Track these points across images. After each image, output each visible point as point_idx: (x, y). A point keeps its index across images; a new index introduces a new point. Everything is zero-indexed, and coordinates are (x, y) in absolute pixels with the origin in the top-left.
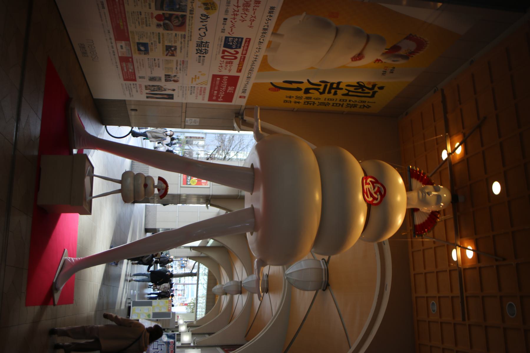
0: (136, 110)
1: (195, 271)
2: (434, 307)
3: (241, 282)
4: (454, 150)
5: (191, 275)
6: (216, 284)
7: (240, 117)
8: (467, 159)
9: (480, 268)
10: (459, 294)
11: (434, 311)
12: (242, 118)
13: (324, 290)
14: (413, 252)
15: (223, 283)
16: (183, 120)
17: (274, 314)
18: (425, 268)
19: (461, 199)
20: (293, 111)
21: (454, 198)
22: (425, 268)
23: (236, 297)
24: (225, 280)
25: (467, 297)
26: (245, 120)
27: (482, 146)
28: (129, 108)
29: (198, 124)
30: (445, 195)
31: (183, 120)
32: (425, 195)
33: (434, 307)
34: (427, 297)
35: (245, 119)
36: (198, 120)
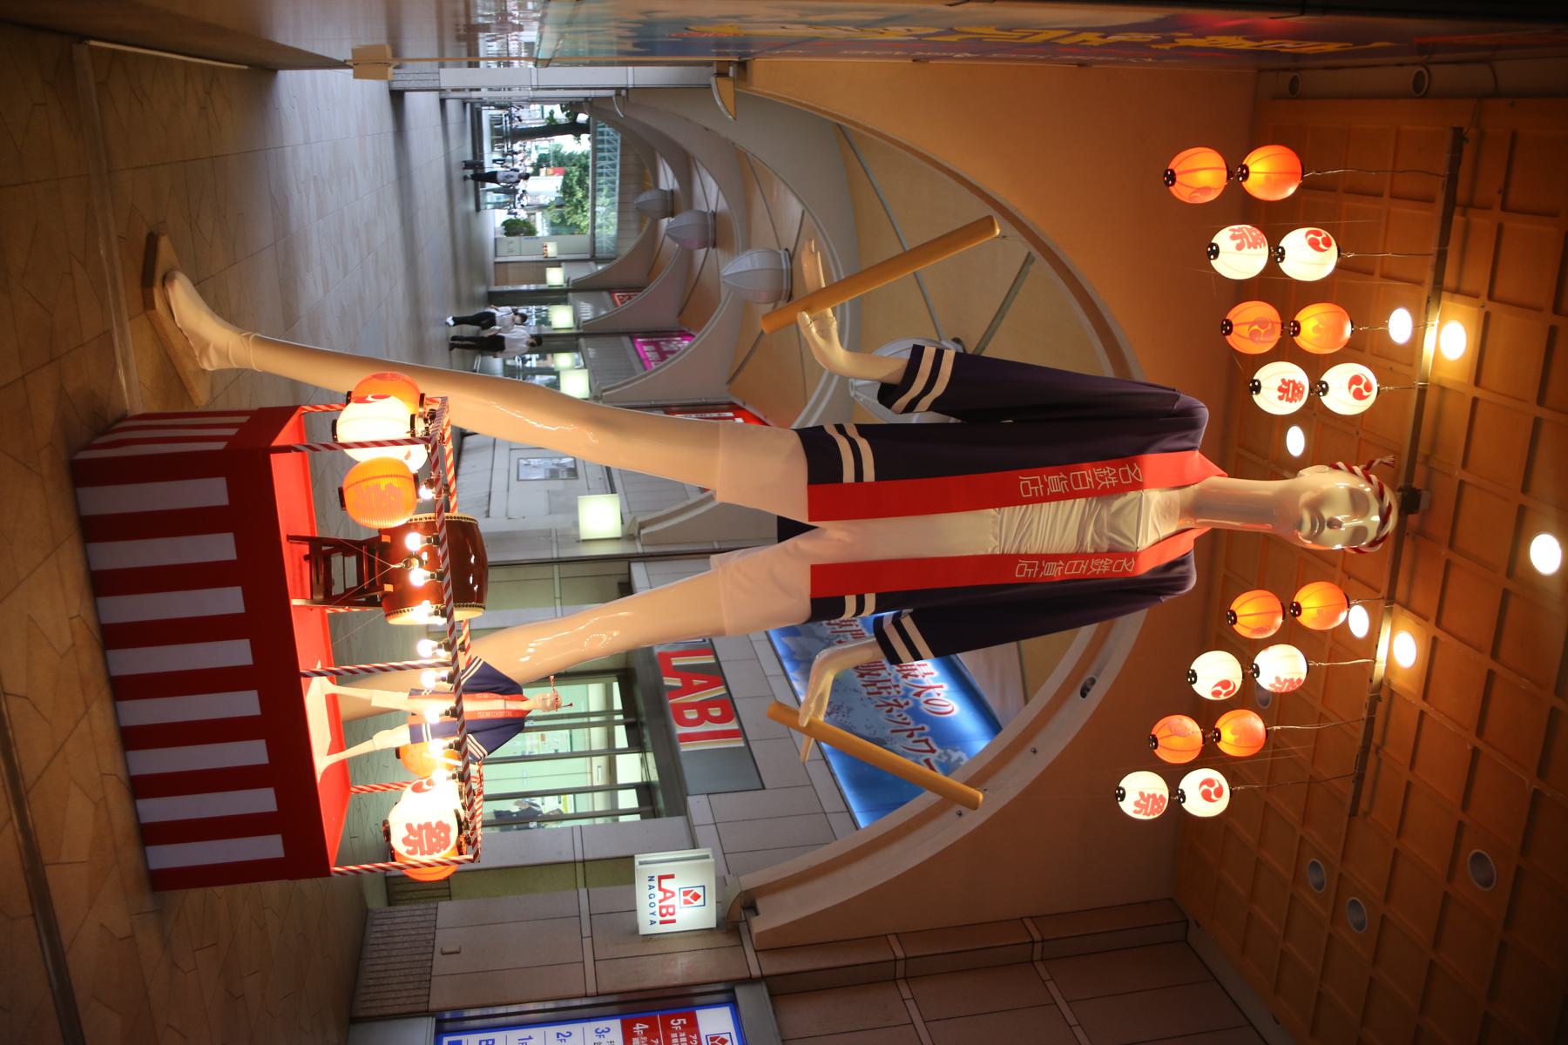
1: (582, 118)
3: (714, 215)
5: (575, 129)
6: (642, 189)
9: (1422, 713)
15: (663, 186)
23: (702, 252)
24: (667, 180)
32: (1321, 529)
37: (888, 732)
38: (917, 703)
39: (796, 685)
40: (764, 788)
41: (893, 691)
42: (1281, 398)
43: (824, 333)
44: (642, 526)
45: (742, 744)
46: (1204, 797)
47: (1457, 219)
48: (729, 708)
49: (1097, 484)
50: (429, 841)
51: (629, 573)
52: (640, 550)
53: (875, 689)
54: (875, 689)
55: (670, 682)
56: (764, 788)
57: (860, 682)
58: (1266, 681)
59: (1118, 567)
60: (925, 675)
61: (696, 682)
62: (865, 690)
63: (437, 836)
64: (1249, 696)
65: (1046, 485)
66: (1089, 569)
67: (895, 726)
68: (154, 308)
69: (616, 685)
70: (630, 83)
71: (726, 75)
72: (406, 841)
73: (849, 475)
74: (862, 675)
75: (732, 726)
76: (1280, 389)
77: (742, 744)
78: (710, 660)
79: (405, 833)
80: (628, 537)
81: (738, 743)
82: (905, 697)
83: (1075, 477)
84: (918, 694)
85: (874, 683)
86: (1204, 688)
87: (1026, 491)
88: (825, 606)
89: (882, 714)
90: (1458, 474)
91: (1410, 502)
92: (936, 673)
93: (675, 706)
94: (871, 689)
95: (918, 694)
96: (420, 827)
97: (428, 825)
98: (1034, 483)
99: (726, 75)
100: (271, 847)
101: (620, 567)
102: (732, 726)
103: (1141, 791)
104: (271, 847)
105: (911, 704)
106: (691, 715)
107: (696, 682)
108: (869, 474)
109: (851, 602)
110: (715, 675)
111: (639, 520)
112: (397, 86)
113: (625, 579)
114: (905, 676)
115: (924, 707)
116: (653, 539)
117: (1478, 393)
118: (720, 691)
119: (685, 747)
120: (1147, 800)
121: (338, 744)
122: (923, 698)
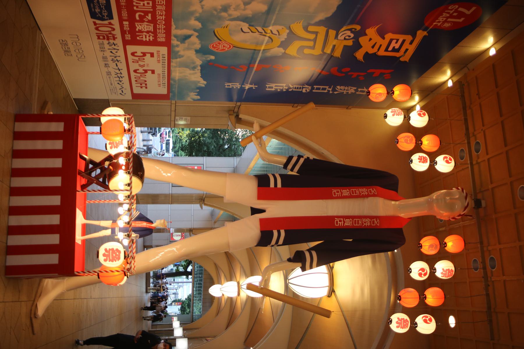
7: (235, 115)
12: (237, 116)
16: (173, 119)
26: (241, 119)
27: (506, 146)
31: (173, 119)
35: (240, 117)
36: (189, 118)
42: (420, 162)
46: (426, 326)
47: (469, 112)
49: (360, 194)
50: (112, 255)
58: (439, 274)
59: (373, 223)
63: (116, 255)
64: (433, 280)
65: (342, 193)
66: (363, 224)
72: (104, 255)
73: (272, 185)
76: (419, 159)
79: (104, 252)
83: (352, 191)
86: (415, 275)
87: (335, 195)
88: (265, 239)
90: (490, 187)
91: (478, 203)
96: (110, 250)
97: (113, 249)
98: (338, 192)
100: (53, 259)
103: (398, 324)
104: (53, 259)
108: (279, 185)
109: (275, 233)
120: (401, 320)
121: (84, 234)
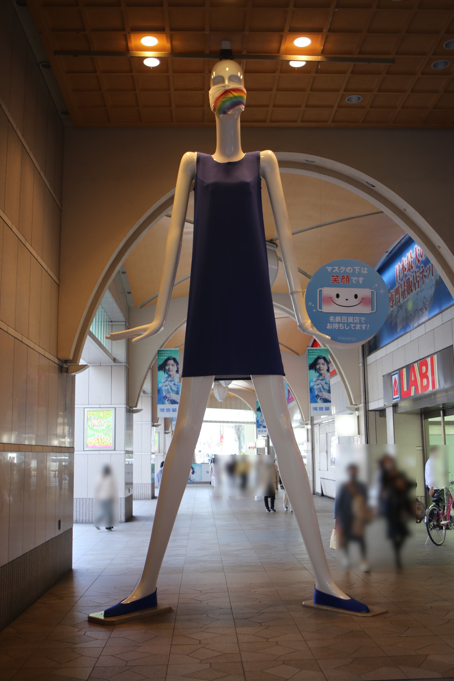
0: (60, 522)
2: (354, 99)
4: (150, 48)
7: (65, 366)
8: (172, 29)
9: (330, 30)
10: (352, 64)
11: (359, 98)
12: (66, 361)
13: (277, 246)
14: (271, 121)
17: (287, 315)
18: (300, 106)
19: (226, 45)
20: (59, 286)
21: (226, 55)
22: (300, 106)
25: (360, 53)
28: (58, 533)
29: (67, 428)
30: (227, 69)
33: (354, 99)
34: (339, 107)
35: (71, 358)
37: (433, 278)
38: (422, 262)
39: (416, 325)
40: (452, 345)
41: (418, 274)
43: (145, 330)
44: (351, 404)
45: (436, 355)
48: (422, 362)
51: (375, 410)
52: (362, 405)
53: (417, 284)
54: (417, 284)
55: (413, 394)
56: (452, 345)
57: (414, 292)
60: (412, 257)
61: (413, 379)
62: (417, 289)
67: (431, 274)
68: (114, 621)
69: (430, 420)
70: (124, 406)
71: (67, 369)
74: (412, 290)
75: (429, 360)
77: (436, 355)
78: (404, 370)
80: (357, 409)
81: (435, 357)
82: (420, 269)
84: (419, 261)
85: (415, 284)
89: (427, 280)
92: (411, 251)
93: (421, 392)
94: (417, 287)
95: (419, 261)
99: (67, 369)
101: (371, 415)
102: (429, 360)
105: (422, 265)
106: (425, 381)
107: (413, 379)
110: (410, 367)
111: (349, 405)
112: (123, 519)
113: (378, 413)
114: (412, 267)
115: (424, 258)
116: (357, 398)
117: (167, 29)
118: (416, 365)
119: (437, 387)
122: (420, 259)
